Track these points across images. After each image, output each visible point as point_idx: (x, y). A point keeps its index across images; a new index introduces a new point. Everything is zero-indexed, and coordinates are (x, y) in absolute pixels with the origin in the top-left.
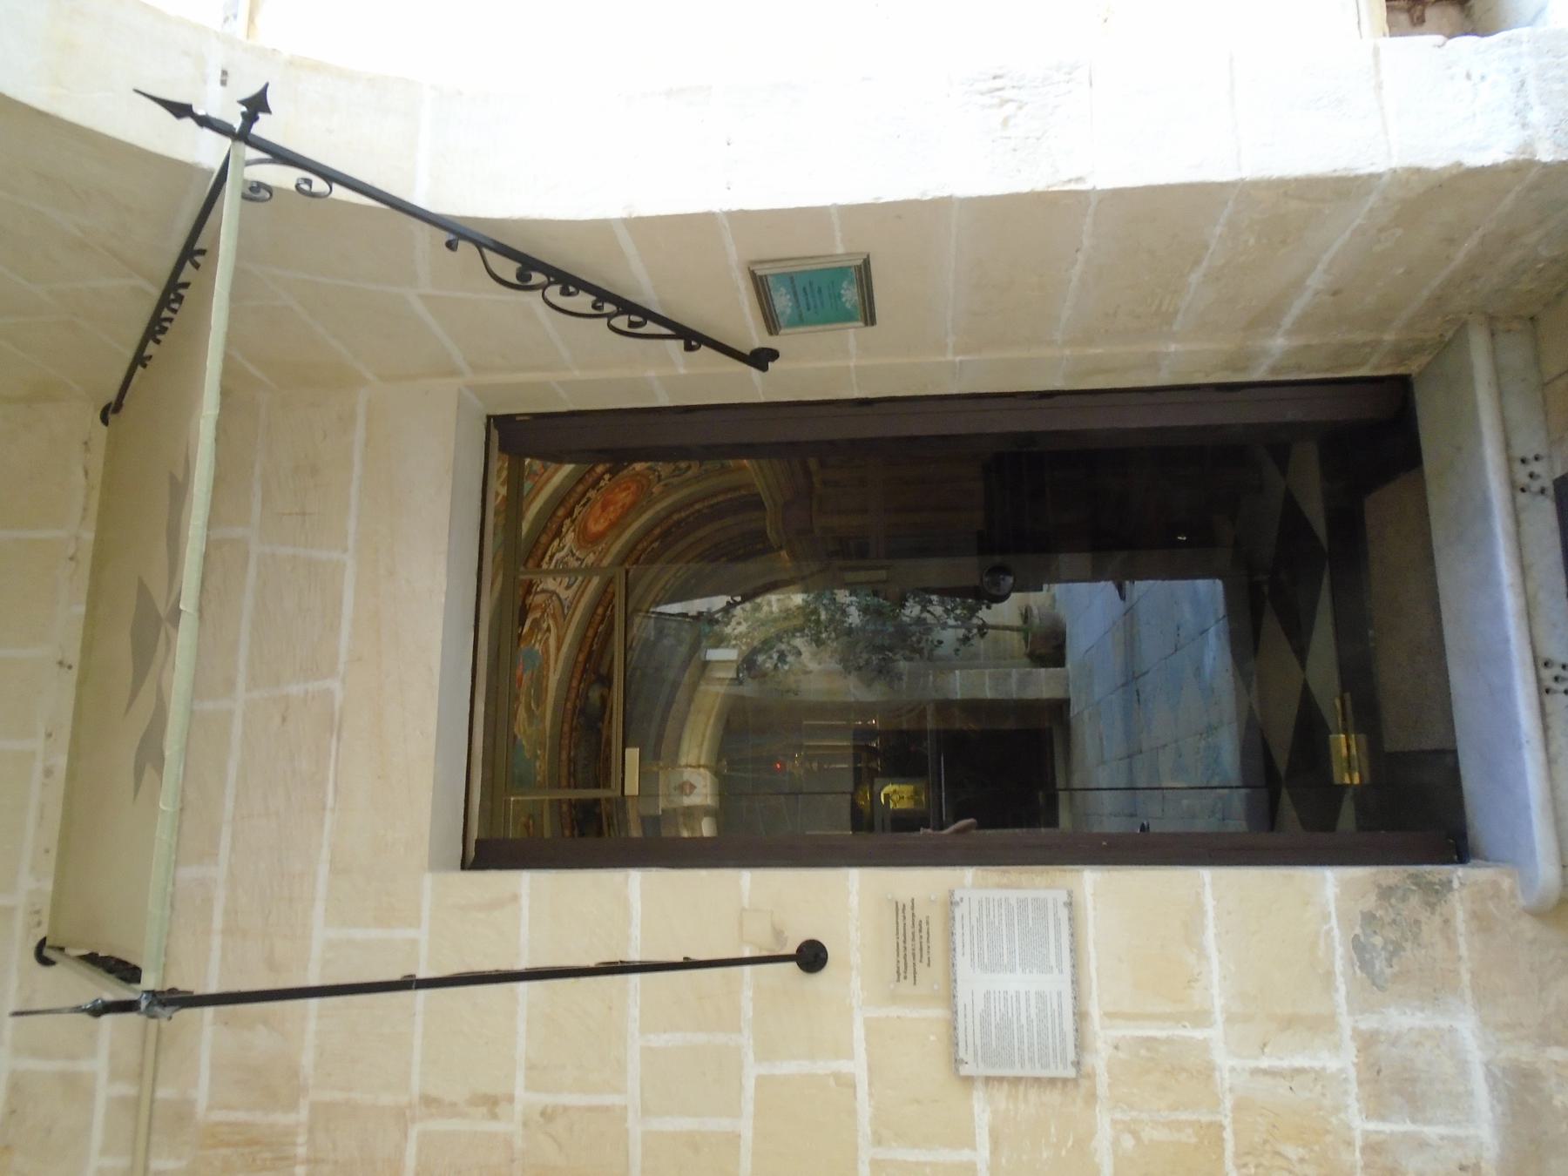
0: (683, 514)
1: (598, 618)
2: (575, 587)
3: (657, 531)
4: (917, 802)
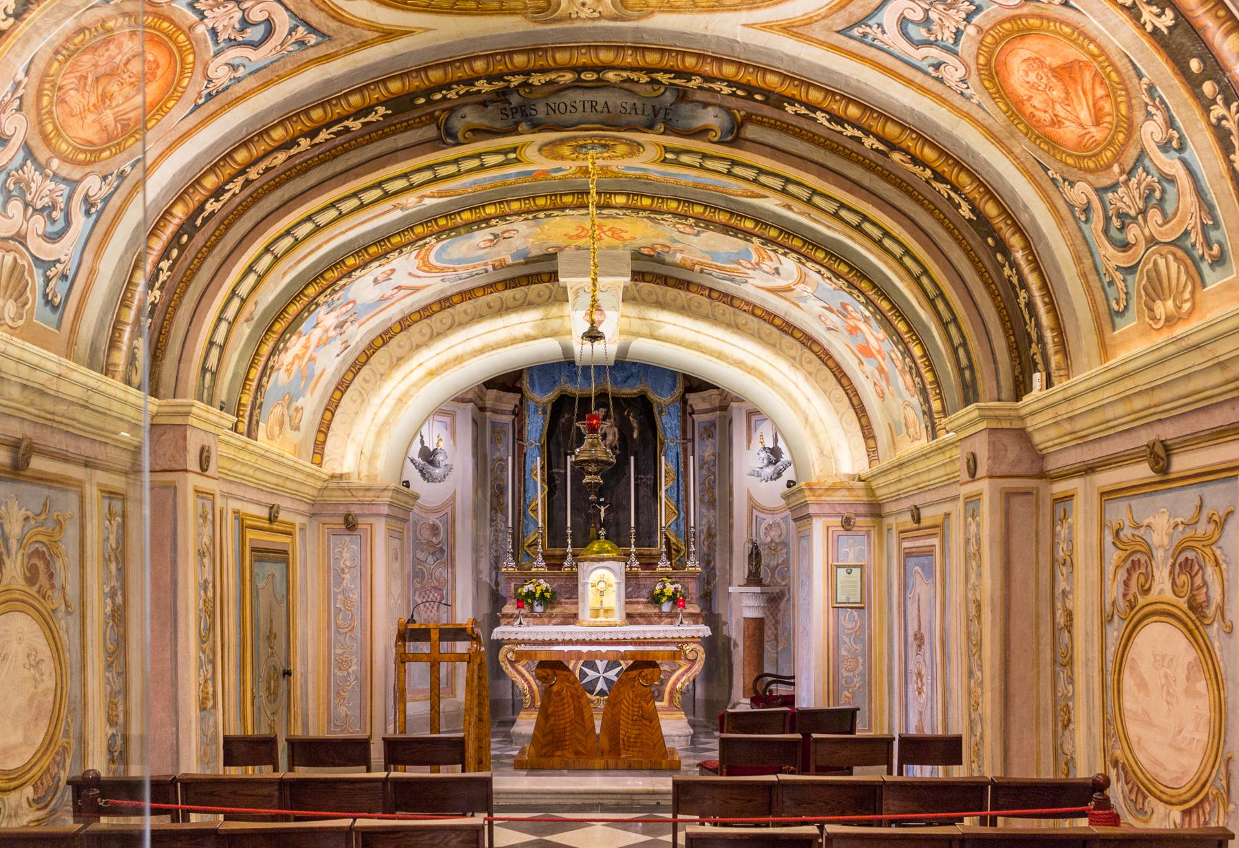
0: (1019, 255)
2: (902, 46)
3: (991, 210)
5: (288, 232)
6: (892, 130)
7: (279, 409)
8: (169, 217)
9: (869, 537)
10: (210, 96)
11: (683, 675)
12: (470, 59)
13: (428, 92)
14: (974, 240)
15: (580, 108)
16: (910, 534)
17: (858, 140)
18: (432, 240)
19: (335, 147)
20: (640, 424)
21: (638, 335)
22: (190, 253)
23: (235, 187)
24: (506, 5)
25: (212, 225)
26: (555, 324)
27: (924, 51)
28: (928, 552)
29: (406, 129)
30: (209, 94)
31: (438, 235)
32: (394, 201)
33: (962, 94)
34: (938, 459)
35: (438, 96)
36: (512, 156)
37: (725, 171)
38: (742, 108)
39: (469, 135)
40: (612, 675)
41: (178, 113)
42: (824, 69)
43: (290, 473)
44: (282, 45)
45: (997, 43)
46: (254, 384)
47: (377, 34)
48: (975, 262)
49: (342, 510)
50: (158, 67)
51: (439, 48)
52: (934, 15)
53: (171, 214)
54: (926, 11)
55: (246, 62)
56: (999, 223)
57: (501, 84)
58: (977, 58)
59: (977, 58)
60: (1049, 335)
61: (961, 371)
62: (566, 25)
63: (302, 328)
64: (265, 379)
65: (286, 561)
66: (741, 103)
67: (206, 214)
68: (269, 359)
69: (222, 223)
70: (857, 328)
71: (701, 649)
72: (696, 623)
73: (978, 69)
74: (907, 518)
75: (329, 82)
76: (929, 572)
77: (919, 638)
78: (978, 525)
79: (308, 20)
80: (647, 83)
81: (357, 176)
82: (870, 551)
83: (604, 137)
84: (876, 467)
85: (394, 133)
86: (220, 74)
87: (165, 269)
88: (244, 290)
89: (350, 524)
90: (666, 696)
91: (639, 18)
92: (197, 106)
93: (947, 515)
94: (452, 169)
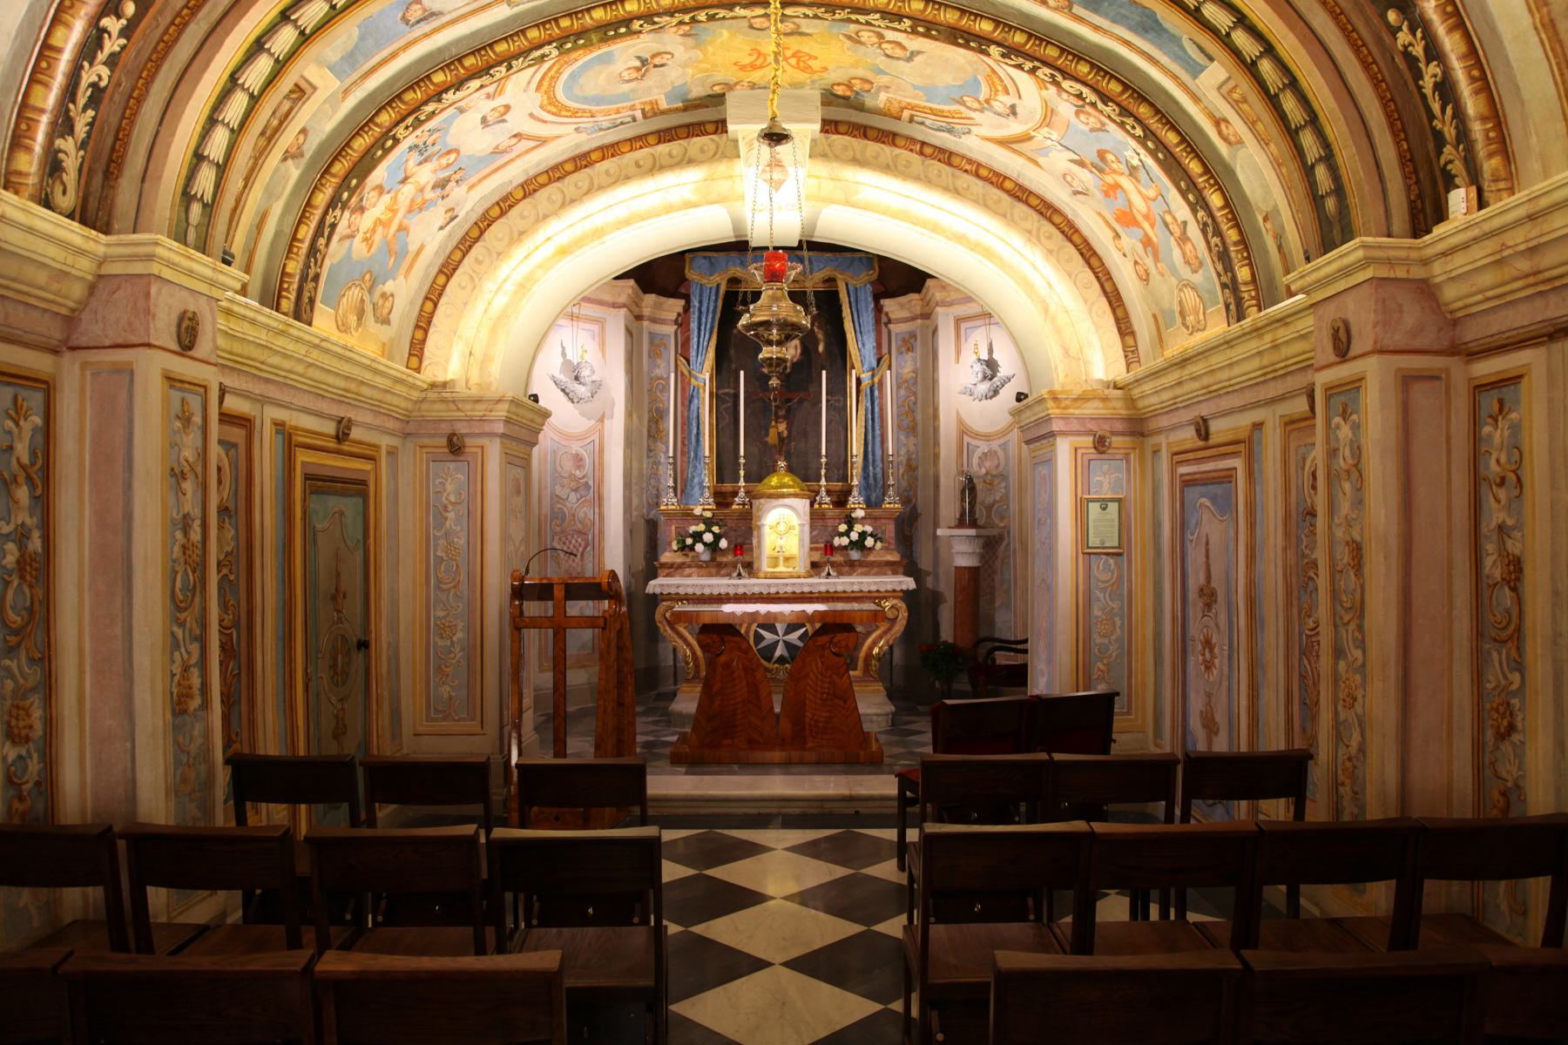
4: (775, 561)
7: (355, 293)
9: (1128, 462)
11: (880, 637)
16: (1191, 456)
20: (826, 335)
21: (831, 201)
26: (722, 187)
28: (1227, 477)
40: (794, 637)
43: (368, 376)
46: (305, 246)
49: (446, 429)
60: (1477, 129)
64: (322, 241)
65: (364, 496)
72: (895, 573)
74: (1190, 433)
76: (1225, 505)
82: (1129, 481)
84: (1138, 371)
89: (455, 447)
90: (860, 664)
93: (1258, 426)
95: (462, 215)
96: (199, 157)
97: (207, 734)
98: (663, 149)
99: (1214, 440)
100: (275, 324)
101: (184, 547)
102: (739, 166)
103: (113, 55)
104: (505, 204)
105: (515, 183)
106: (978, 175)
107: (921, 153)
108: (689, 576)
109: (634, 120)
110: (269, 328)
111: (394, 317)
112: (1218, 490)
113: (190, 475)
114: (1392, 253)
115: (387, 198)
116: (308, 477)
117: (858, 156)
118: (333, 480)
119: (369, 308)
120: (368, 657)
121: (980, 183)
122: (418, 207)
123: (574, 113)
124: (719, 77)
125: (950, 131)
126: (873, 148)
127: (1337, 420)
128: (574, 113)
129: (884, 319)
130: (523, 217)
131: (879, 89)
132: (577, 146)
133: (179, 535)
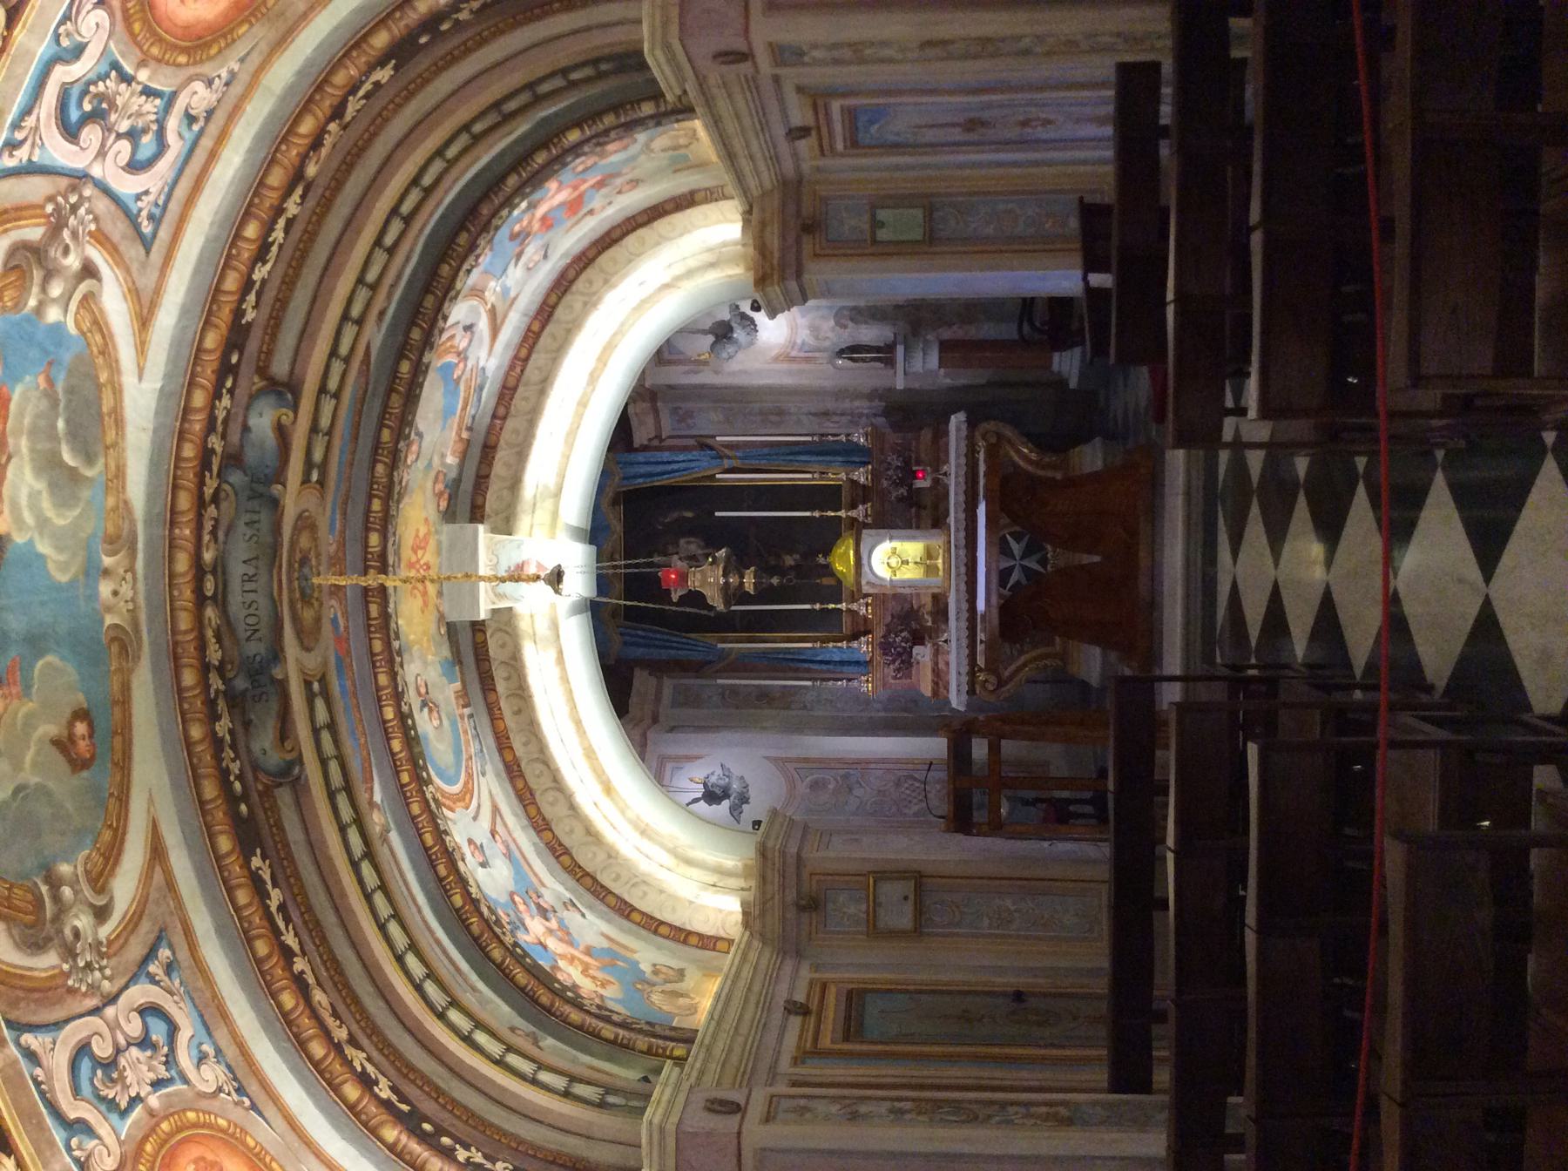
1: (247, 251)
2: (165, 166)
3: (381, 40)
4: (930, 570)
5: (418, 988)
6: (276, 178)
8: (400, 1147)
10: (240, 1090)
11: (1019, 452)
12: (189, 744)
13: (232, 800)
14: (422, 63)
15: (252, 596)
16: (825, 142)
17: (290, 223)
18: (429, 791)
19: (305, 922)
21: (555, 515)
22: (446, 1119)
23: (358, 1058)
24: (118, 696)
25: (411, 1091)
26: (543, 629)
27: (171, 137)
28: (851, 115)
29: (282, 829)
30: (238, 1090)
31: (421, 781)
32: (377, 843)
33: (227, 84)
34: (722, 105)
35: (238, 786)
36: (316, 686)
37: (333, 402)
38: (249, 381)
39: (288, 745)
40: (1016, 548)
41: (263, 1133)
42: (197, 271)
43: (741, 984)
44: (172, 994)
45: (161, 40)
46: (621, 1032)
47: (158, 869)
48: (452, 60)
49: (791, 914)
50: (203, 1159)
51: (175, 786)
52: (124, 126)
53: (395, 1144)
54: (119, 136)
55: (195, 1042)
56: (398, 28)
57: (221, 705)
58: (179, 66)
59: (179, 66)
61: (601, 76)
62: (143, 617)
63: (545, 964)
64: (615, 1017)
65: (863, 992)
66: (243, 382)
67: (394, 1098)
68: (588, 1012)
69: (406, 1076)
70: (544, 219)
71: (985, 426)
73: (195, 63)
74: (803, 145)
75: (220, 931)
76: (877, 114)
77: (972, 125)
78: (815, 46)
79: (139, 958)
80: (217, 508)
81: (344, 895)
83: (290, 565)
84: (730, 189)
85: (287, 845)
86: (210, 1077)
87: (467, 1154)
88: (495, 1049)
91: (133, 522)
92: (254, 1107)
93: (800, 90)
94: (334, 766)
95: (568, 895)
96: (566, 1094)
97: (1095, 1103)
98: (501, 686)
99: (809, 120)
100: (701, 1056)
101: (919, 1113)
102: (521, 609)
103: (486, 1156)
104: (558, 851)
105: (537, 840)
106: (527, 359)
107: (504, 418)
108: (947, 664)
109: (471, 716)
110: (705, 1061)
111: (675, 964)
112: (863, 119)
113: (854, 1108)
114: (658, 23)
115: (561, 963)
116: (846, 1039)
117: (508, 484)
118: (848, 1018)
119: (669, 987)
120: (1034, 994)
121: (534, 356)
122: (566, 936)
123: (470, 776)
124: (433, 627)
125: (481, 388)
126: (499, 468)
127: (806, 59)
128: (470, 776)
129: (656, 443)
130: (572, 831)
131: (443, 464)
132: (498, 775)
133: (908, 1116)
